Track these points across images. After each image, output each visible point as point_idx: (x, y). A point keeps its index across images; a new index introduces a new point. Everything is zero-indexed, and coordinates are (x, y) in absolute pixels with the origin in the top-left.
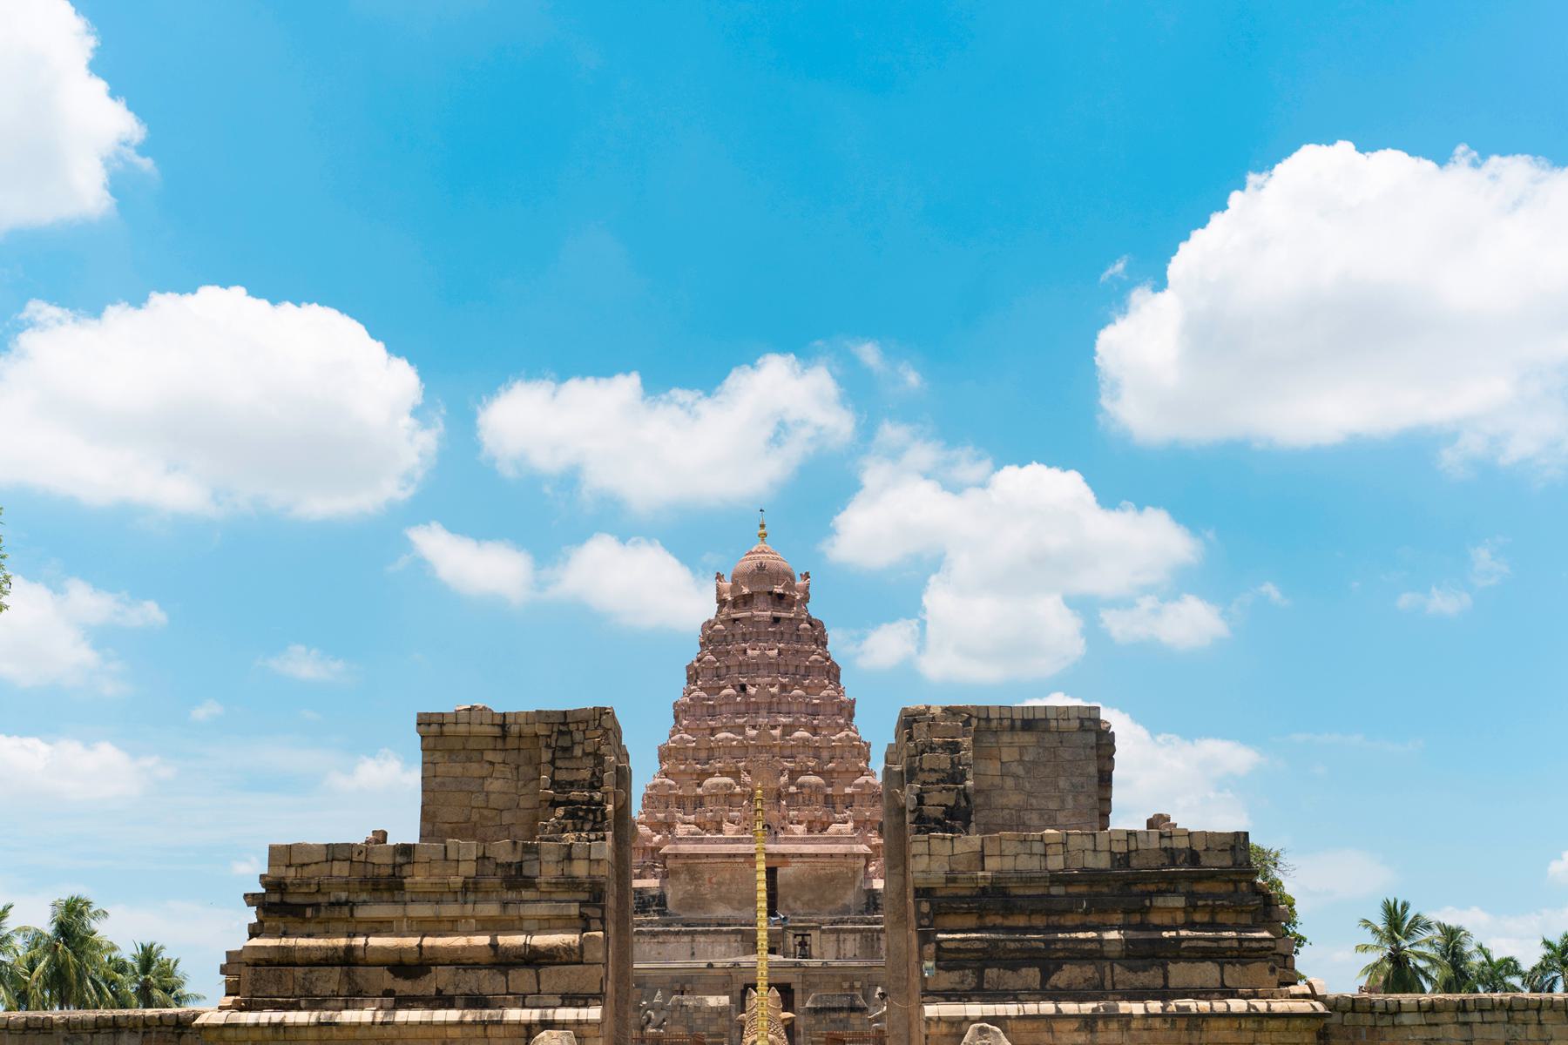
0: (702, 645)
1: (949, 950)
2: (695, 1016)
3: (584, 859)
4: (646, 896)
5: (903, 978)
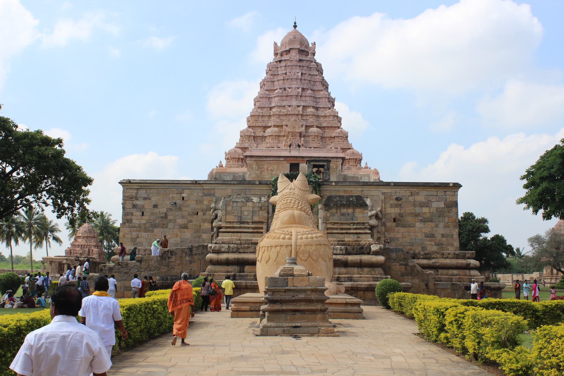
0: (267, 73)
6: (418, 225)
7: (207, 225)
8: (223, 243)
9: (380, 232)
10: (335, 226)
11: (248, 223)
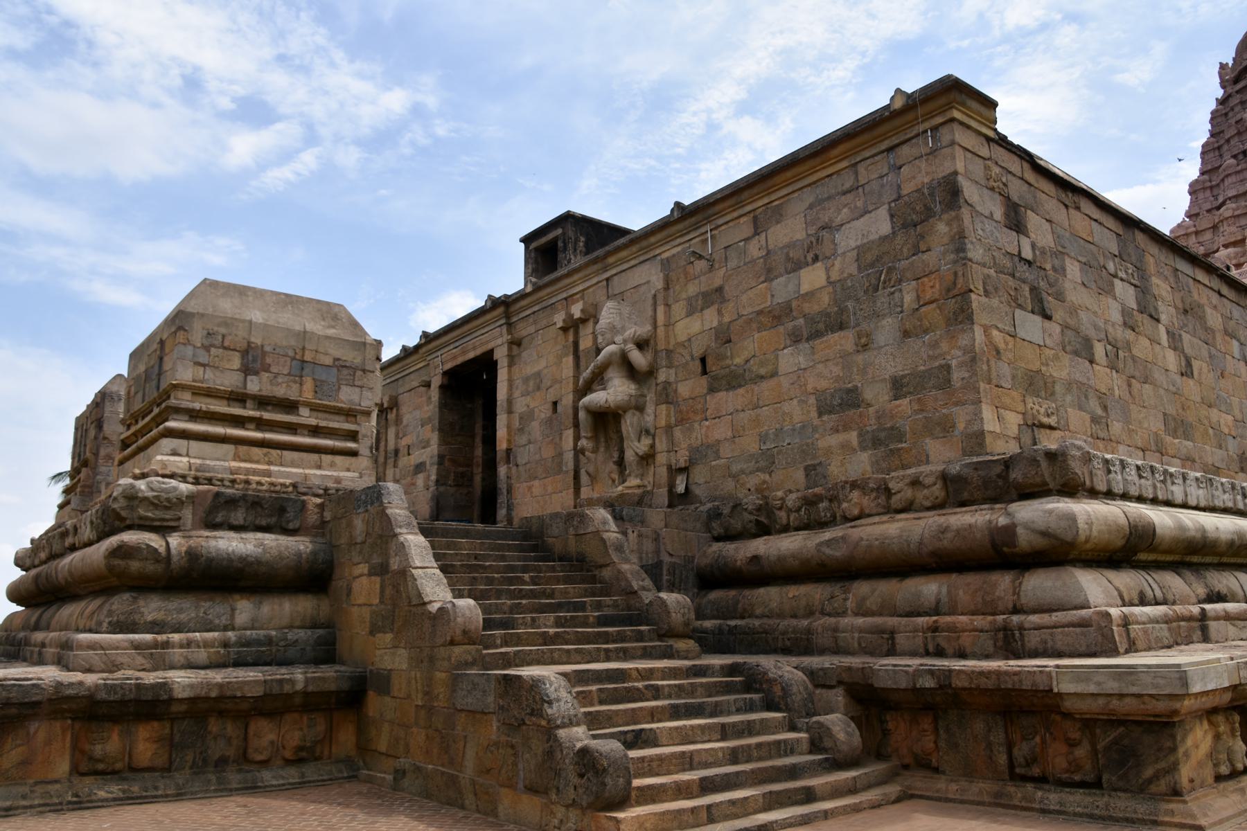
6: (790, 359)
9: (652, 431)
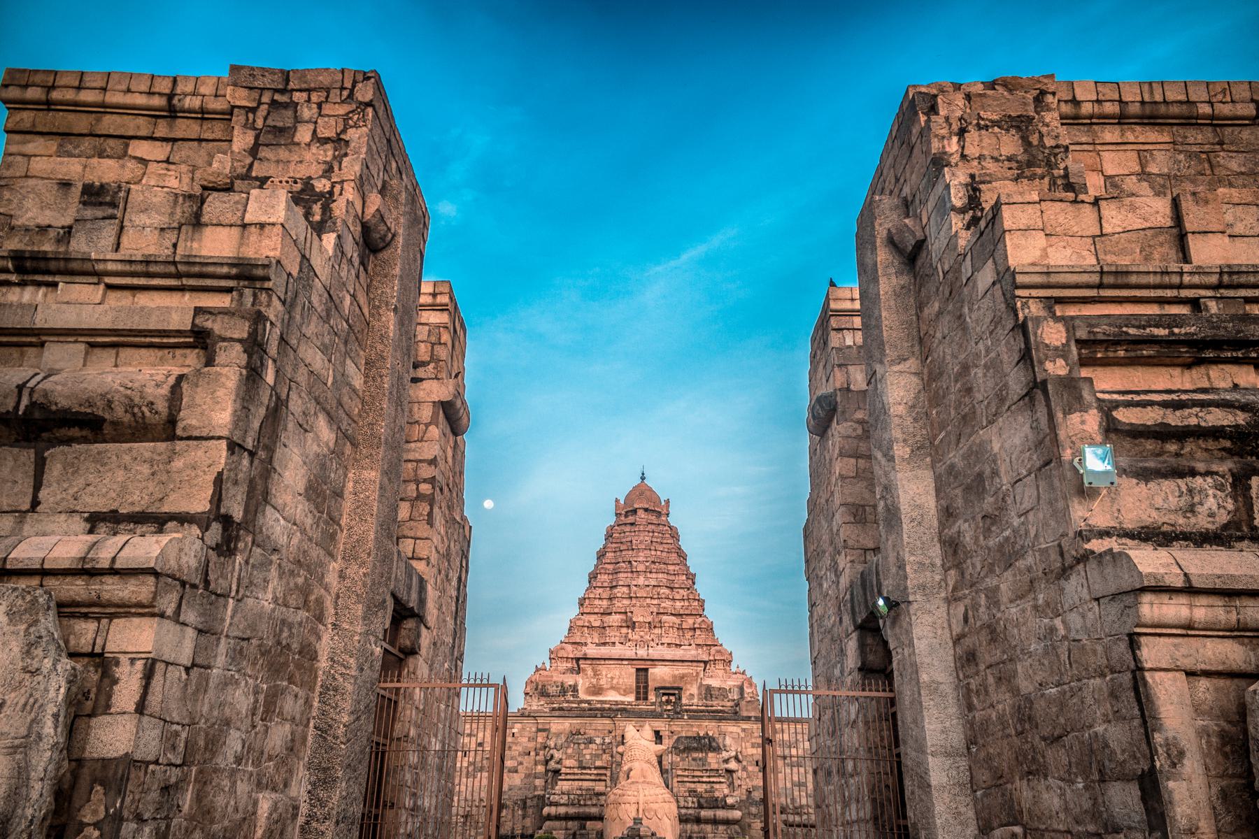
1: (1137, 433)
2: (584, 752)
3: (231, 226)
4: (566, 686)
5: (933, 565)
7: (540, 768)
8: (563, 793)
10: (686, 773)
11: (590, 768)
